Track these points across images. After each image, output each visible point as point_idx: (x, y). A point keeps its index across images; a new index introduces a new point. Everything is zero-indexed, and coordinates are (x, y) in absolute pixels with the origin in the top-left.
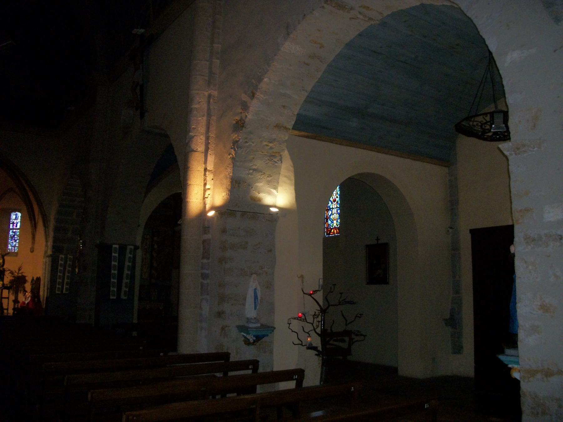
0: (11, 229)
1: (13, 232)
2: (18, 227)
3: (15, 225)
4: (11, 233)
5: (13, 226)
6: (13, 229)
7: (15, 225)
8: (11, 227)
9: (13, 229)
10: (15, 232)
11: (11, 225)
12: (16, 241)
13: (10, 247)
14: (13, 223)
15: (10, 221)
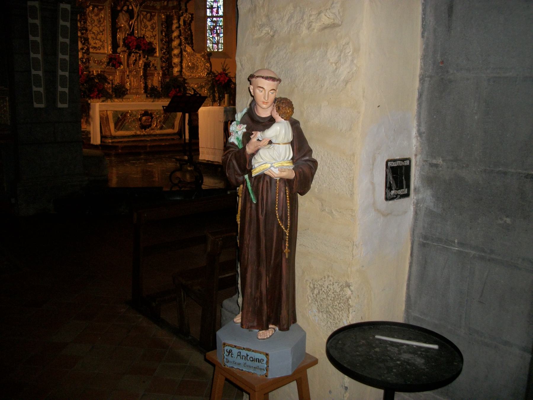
0: (209, 17)
1: (212, 21)
2: (221, 13)
3: (215, 10)
4: (209, 23)
5: (212, 12)
6: (213, 17)
7: (215, 10)
8: (209, 13)
9: (213, 17)
10: (216, 22)
11: (208, 11)
12: (218, 35)
13: (209, 44)
14: (212, 8)
15: (206, 5)
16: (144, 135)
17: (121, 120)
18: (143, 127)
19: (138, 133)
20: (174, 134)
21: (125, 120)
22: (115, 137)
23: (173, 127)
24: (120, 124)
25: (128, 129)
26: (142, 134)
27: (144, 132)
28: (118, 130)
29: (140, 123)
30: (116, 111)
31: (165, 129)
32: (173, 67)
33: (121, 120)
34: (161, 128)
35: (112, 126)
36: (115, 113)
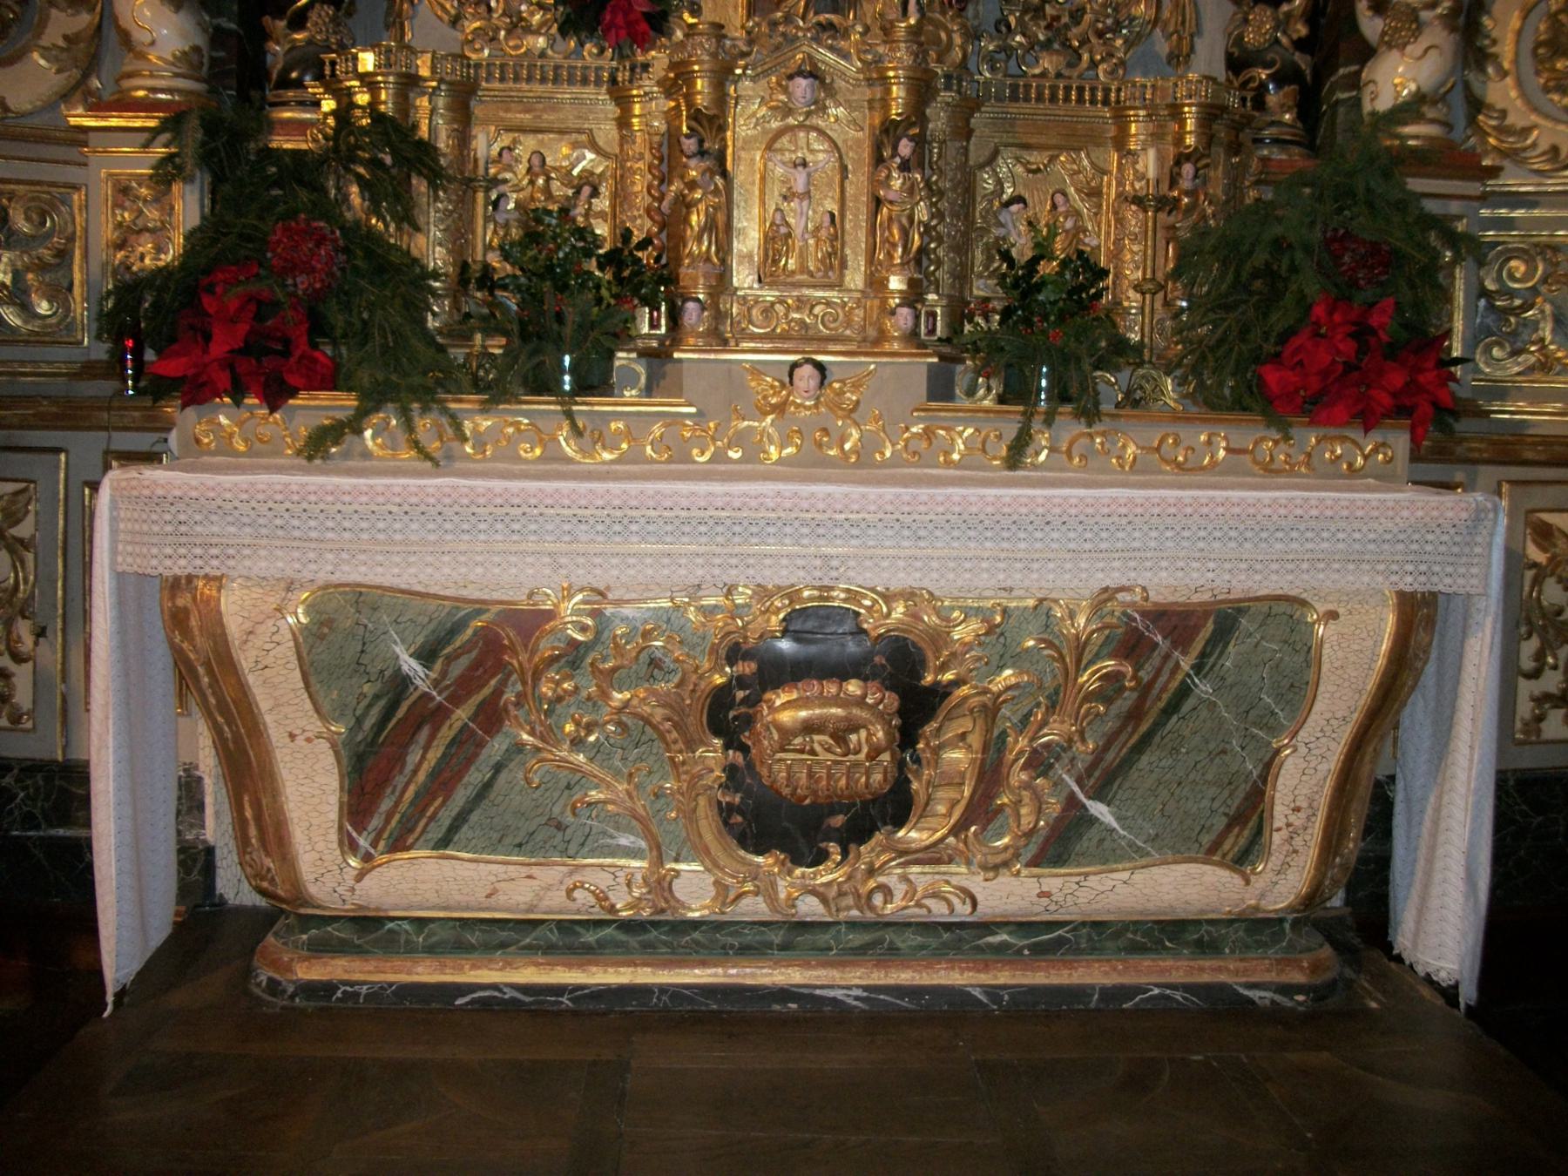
16: (794, 937)
17: (429, 715)
18: (773, 823)
19: (695, 889)
20: (1257, 928)
21: (491, 717)
22: (369, 930)
23: (1242, 831)
24: (423, 759)
25: (550, 834)
26: (754, 908)
27: (801, 889)
28: (398, 844)
29: (713, 753)
30: (361, 597)
31: (1109, 854)
32: (1366, 53)
33: (429, 715)
34: (1061, 843)
35: (310, 787)
36: (338, 637)
